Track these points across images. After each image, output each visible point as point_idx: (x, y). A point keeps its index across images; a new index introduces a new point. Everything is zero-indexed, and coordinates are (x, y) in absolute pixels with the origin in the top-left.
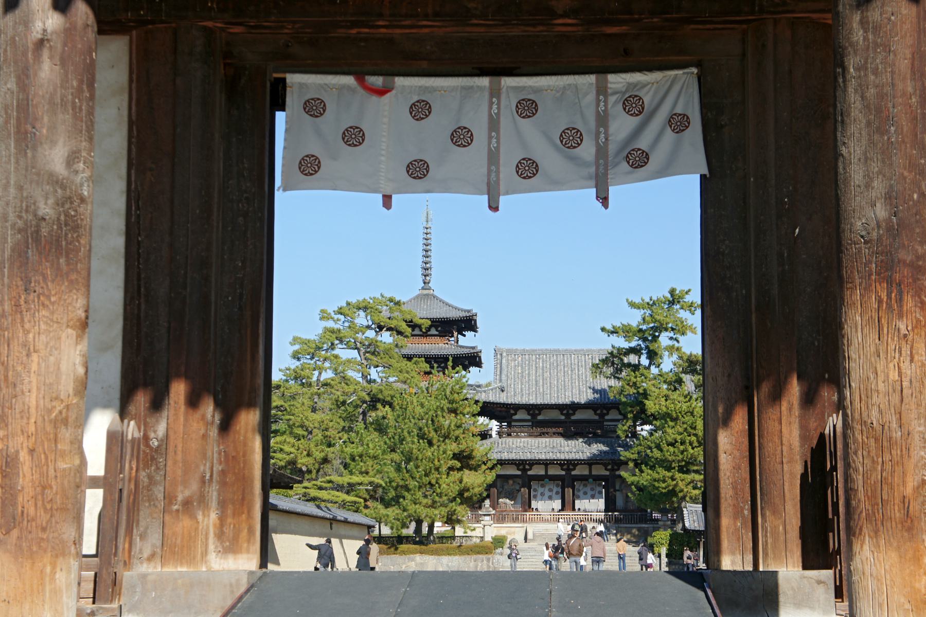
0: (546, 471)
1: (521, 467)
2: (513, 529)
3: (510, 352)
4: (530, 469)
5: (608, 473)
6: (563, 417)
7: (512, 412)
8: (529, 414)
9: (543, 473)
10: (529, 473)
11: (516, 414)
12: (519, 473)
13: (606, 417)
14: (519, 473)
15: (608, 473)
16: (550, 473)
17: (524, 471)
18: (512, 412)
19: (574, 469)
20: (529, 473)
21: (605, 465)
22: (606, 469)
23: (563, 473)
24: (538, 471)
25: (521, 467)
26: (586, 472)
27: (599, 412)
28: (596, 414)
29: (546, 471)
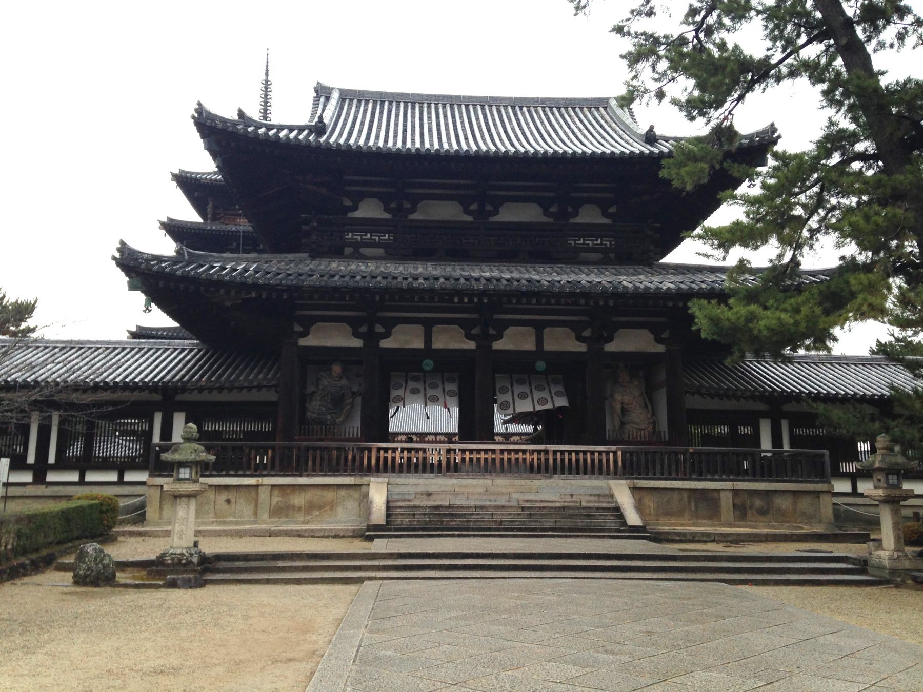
0: (428, 339)
1: (364, 329)
2: (329, 495)
3: (347, 96)
4: (387, 335)
5: (582, 348)
6: (469, 219)
7: (347, 203)
8: (386, 210)
9: (419, 344)
10: (385, 344)
11: (355, 208)
12: (357, 343)
13: (572, 221)
14: (357, 343)
15: (582, 348)
16: (437, 344)
17: (371, 338)
18: (347, 203)
19: (500, 336)
20: (385, 344)
21: (577, 329)
22: (580, 339)
23: (472, 345)
25: (364, 329)
26: (529, 345)
27: (553, 209)
28: (546, 213)
29: (428, 339)
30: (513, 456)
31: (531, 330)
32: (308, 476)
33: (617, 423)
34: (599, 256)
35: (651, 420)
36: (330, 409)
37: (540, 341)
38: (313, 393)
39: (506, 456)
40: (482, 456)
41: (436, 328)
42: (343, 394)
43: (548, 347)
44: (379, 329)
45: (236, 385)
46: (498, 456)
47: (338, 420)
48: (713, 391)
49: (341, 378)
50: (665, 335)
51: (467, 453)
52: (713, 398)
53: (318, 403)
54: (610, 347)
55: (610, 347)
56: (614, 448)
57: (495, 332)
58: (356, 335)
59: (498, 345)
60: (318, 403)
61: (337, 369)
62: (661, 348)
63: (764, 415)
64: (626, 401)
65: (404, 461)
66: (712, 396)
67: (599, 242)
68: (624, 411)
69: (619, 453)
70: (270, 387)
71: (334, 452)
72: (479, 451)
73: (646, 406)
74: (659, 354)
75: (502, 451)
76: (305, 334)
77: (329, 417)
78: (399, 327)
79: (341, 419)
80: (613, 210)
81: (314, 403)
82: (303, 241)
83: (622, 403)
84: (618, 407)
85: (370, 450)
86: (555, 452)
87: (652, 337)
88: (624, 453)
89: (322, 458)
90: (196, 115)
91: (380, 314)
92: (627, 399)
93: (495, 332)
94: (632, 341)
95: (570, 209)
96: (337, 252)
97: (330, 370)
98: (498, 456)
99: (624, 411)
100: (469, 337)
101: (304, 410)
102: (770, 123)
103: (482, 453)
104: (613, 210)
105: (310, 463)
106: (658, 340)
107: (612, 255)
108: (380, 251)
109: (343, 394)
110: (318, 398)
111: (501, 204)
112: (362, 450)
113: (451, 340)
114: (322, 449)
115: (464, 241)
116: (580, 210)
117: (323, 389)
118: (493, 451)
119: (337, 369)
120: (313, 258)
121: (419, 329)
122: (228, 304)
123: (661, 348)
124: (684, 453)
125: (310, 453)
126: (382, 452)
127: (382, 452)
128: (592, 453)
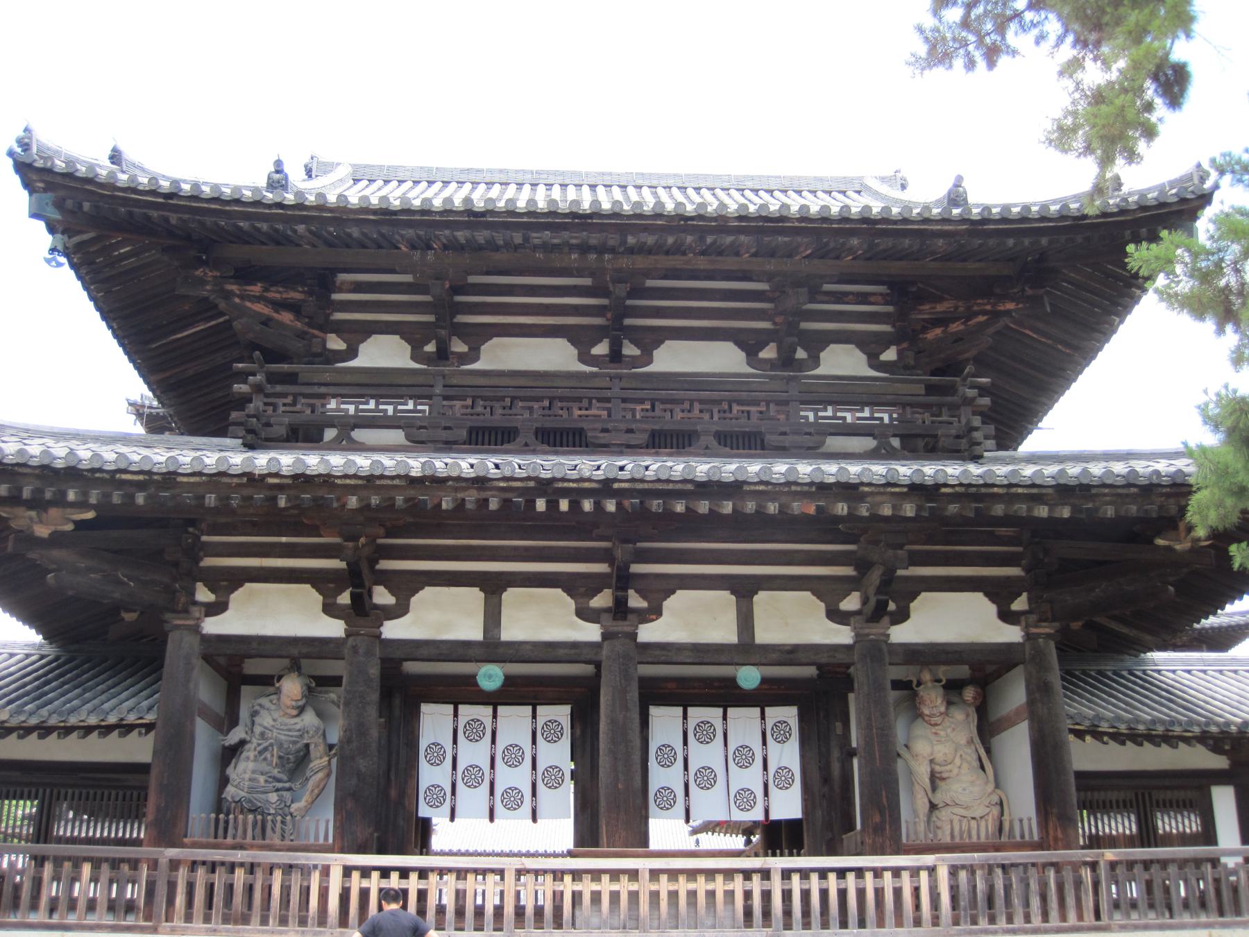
0: (493, 618)
4: (400, 610)
5: (842, 635)
9: (471, 630)
10: (393, 630)
12: (334, 628)
14: (334, 628)
15: (842, 635)
18: (336, 343)
19: (655, 612)
20: (393, 630)
21: (828, 592)
22: (835, 615)
23: (591, 632)
24: (441, 617)
26: (724, 632)
29: (493, 618)
30: (683, 886)
31: (725, 598)
32: (173, 930)
33: (922, 805)
34: (869, 443)
35: (995, 799)
36: (279, 781)
37: (746, 621)
38: (242, 743)
39: (664, 886)
40: (606, 886)
41: (511, 595)
42: (307, 746)
43: (765, 634)
44: (382, 596)
45: (73, 720)
46: (644, 887)
47: (294, 806)
48: (1123, 728)
49: (301, 710)
50: (1020, 604)
51: (568, 878)
52: (1123, 743)
53: (251, 765)
54: (901, 634)
55: (901, 634)
56: (928, 859)
57: (644, 604)
58: (330, 609)
59: (648, 633)
60: (251, 765)
61: (292, 687)
62: (1012, 634)
63: (1219, 777)
64: (939, 757)
65: (449, 900)
66: (1118, 738)
67: (866, 414)
68: (935, 779)
69: (943, 873)
70: (149, 727)
71: (240, 876)
72: (596, 874)
73: (982, 768)
74: (1009, 646)
75: (655, 874)
76: (218, 608)
77: (273, 797)
78: (428, 592)
79: (302, 804)
80: (890, 355)
81: (242, 765)
82: (234, 415)
83: (932, 761)
84: (923, 771)
85: (326, 871)
86: (786, 874)
87: (992, 609)
88: (954, 871)
89: (210, 888)
90: (19, 150)
91: (386, 565)
92: (942, 751)
93: (644, 604)
94: (952, 618)
95: (801, 354)
96: (304, 435)
97: (278, 692)
98: (644, 887)
99: (935, 779)
100: (584, 614)
101: (224, 781)
102: (1194, 163)
103: (605, 878)
104: (890, 355)
105: (180, 900)
106: (1006, 616)
107: (896, 442)
108: (397, 436)
109: (307, 746)
110: (252, 754)
111: (658, 343)
112: (306, 871)
113: (544, 618)
114: (212, 867)
115: (577, 413)
116: (822, 355)
117: (262, 734)
118: (634, 874)
119: (292, 687)
120: (250, 447)
121: (474, 596)
122: (42, 531)
123: (1012, 634)
124: (1094, 866)
125: (182, 875)
126: (356, 875)
127: (356, 875)
128: (878, 872)
